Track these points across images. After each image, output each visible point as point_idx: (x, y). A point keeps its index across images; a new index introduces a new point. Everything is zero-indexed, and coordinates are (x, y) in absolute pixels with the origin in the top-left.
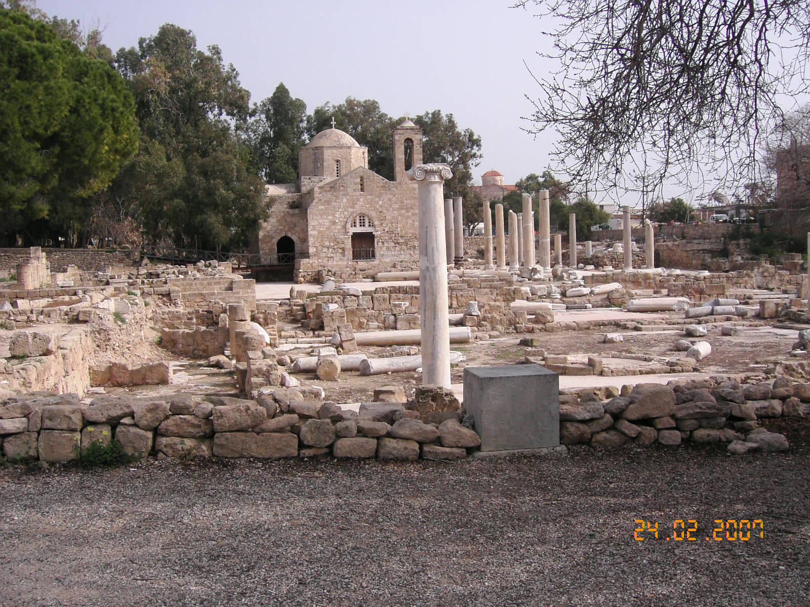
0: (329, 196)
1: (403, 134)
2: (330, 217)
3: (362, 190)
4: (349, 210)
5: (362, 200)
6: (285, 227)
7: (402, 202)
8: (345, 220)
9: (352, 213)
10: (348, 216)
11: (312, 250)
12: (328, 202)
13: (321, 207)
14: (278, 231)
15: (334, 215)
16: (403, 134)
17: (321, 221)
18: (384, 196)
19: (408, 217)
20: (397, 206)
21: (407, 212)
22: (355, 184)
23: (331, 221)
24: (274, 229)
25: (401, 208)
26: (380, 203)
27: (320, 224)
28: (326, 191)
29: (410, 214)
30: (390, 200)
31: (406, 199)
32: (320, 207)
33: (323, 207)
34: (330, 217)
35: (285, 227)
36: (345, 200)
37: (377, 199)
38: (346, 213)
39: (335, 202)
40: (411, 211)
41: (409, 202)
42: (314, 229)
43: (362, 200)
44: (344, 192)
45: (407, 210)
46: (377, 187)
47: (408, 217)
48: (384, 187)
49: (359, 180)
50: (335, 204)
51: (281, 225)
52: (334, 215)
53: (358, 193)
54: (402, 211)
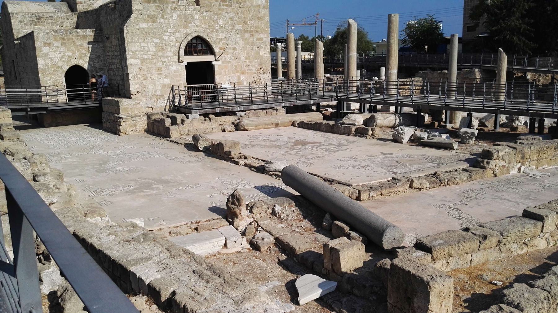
0: (154, 8)
2: (157, 40)
4: (182, 30)
5: (197, 17)
6: (73, 54)
7: (246, 23)
8: (178, 44)
9: (187, 35)
10: (181, 40)
11: (134, 87)
12: (152, 18)
13: (143, 25)
14: (66, 58)
15: (161, 38)
19: (252, 43)
21: (252, 35)
23: (157, 45)
24: (59, 56)
25: (246, 32)
26: (220, 22)
27: (143, 49)
30: (231, 18)
31: (250, 20)
32: (142, 25)
33: (145, 25)
35: (73, 54)
36: (175, 17)
37: (216, 17)
38: (177, 35)
39: (162, 17)
40: (256, 35)
43: (197, 17)
44: (175, 5)
45: (252, 33)
47: (252, 43)
50: (161, 21)
51: (68, 51)
52: (161, 38)
54: (247, 35)
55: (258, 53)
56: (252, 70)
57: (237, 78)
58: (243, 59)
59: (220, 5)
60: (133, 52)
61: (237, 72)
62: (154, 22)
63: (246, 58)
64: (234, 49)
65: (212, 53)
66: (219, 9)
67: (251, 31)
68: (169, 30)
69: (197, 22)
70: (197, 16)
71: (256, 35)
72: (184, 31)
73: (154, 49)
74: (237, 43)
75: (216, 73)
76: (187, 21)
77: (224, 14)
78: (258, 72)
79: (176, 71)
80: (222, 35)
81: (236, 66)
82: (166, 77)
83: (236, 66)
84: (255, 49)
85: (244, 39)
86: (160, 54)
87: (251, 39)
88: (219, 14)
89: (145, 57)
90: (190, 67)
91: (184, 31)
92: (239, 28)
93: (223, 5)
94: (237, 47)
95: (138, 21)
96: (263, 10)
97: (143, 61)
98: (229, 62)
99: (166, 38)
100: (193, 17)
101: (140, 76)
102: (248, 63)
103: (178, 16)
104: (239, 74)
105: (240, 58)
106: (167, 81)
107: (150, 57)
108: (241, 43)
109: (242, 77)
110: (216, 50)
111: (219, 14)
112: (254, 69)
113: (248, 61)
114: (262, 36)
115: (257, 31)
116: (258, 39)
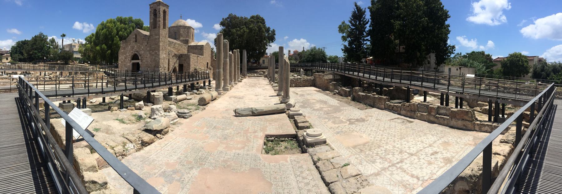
2: (125, 55)
3: (136, 41)
7: (151, 47)
12: (124, 48)
13: (122, 51)
21: (153, 52)
22: (134, 38)
25: (150, 50)
26: (142, 47)
28: (124, 43)
29: (154, 53)
31: (152, 45)
34: (125, 55)
36: (130, 47)
38: (130, 53)
41: (154, 46)
43: (135, 46)
44: (130, 43)
46: (141, 39)
48: (144, 39)
49: (134, 36)
50: (126, 49)
53: (134, 43)
54: (151, 52)
55: (154, 59)
56: (152, 66)
57: (147, 69)
58: (149, 62)
59: (142, 41)
62: (125, 49)
63: (150, 61)
64: (146, 57)
65: (138, 59)
66: (142, 42)
67: (152, 50)
68: (128, 52)
69: (135, 48)
71: (155, 52)
72: (132, 52)
73: (124, 58)
74: (147, 55)
77: (144, 44)
79: (129, 65)
80: (142, 52)
82: (126, 67)
83: (147, 64)
84: (154, 57)
85: (150, 54)
86: (125, 60)
87: (152, 53)
88: (142, 44)
89: (122, 61)
90: (133, 64)
91: (132, 52)
92: (149, 49)
94: (147, 57)
97: (122, 62)
98: (144, 63)
99: (127, 55)
100: (134, 46)
102: (151, 63)
103: (131, 47)
105: (148, 61)
106: (126, 69)
108: (149, 55)
110: (140, 58)
111: (142, 44)
113: (151, 62)
114: (157, 51)
115: (155, 50)
116: (155, 53)
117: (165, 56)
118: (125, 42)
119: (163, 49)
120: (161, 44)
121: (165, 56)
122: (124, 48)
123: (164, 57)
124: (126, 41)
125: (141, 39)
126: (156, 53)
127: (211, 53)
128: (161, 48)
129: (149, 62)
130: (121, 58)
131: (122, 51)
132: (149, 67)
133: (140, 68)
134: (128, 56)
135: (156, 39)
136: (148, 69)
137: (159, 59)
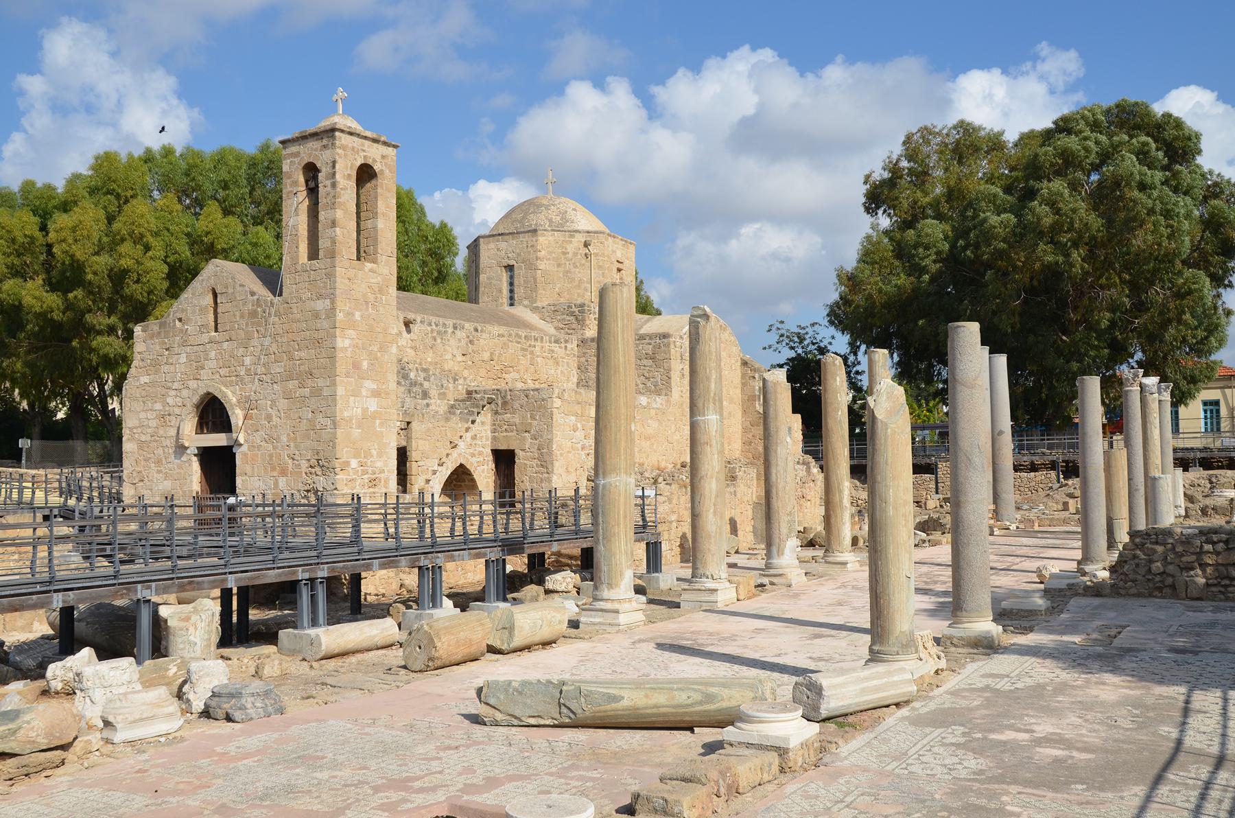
0: (158, 347)
1: (297, 155)
2: (158, 406)
7: (291, 359)
13: (145, 379)
16: (297, 155)
17: (142, 415)
18: (255, 342)
20: (277, 369)
26: (247, 360)
28: (152, 337)
34: (158, 406)
36: (183, 359)
40: (310, 383)
42: (132, 439)
48: (253, 314)
54: (292, 384)
58: (284, 439)
60: (131, 429)
61: (273, 469)
62: (157, 372)
70: (214, 353)
72: (193, 384)
75: (238, 471)
76: (198, 365)
78: (313, 470)
81: (271, 456)
83: (271, 456)
89: (143, 438)
92: (278, 370)
93: (253, 324)
95: (139, 373)
96: (325, 323)
97: (142, 445)
99: (169, 400)
101: (135, 474)
104: (275, 474)
105: (278, 439)
107: (148, 438)
108: (283, 404)
109: (282, 482)
112: (304, 464)
113: (292, 445)
114: (321, 383)
117: (373, 405)
118: (156, 328)
119: (357, 366)
120: (343, 342)
121: (373, 405)
122: (156, 364)
123: (365, 410)
124: (162, 325)
125: (242, 316)
126: (317, 392)
127: (744, 376)
128: (341, 368)
129: (284, 439)
130: (137, 423)
131: (145, 379)
132: (283, 472)
133: (239, 481)
134: (177, 411)
135: (316, 316)
136: (276, 484)
137: (335, 425)
